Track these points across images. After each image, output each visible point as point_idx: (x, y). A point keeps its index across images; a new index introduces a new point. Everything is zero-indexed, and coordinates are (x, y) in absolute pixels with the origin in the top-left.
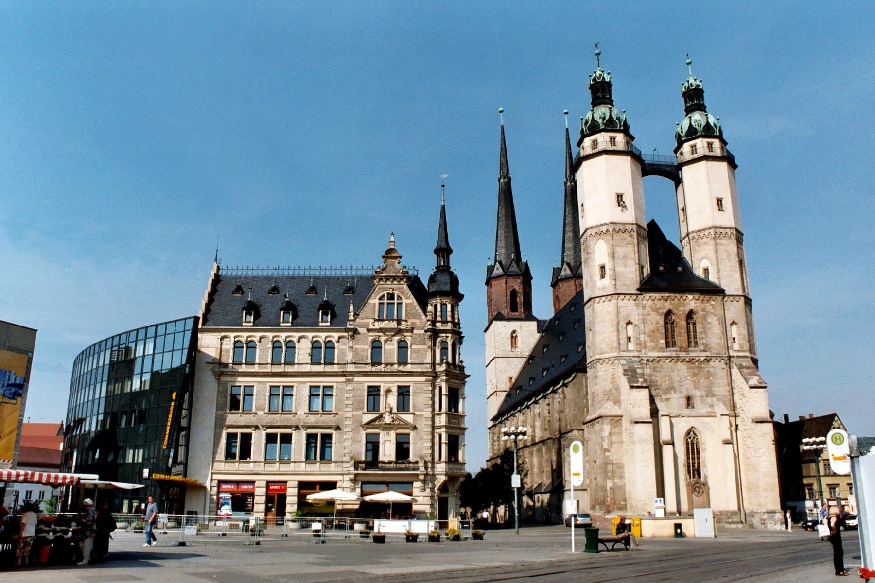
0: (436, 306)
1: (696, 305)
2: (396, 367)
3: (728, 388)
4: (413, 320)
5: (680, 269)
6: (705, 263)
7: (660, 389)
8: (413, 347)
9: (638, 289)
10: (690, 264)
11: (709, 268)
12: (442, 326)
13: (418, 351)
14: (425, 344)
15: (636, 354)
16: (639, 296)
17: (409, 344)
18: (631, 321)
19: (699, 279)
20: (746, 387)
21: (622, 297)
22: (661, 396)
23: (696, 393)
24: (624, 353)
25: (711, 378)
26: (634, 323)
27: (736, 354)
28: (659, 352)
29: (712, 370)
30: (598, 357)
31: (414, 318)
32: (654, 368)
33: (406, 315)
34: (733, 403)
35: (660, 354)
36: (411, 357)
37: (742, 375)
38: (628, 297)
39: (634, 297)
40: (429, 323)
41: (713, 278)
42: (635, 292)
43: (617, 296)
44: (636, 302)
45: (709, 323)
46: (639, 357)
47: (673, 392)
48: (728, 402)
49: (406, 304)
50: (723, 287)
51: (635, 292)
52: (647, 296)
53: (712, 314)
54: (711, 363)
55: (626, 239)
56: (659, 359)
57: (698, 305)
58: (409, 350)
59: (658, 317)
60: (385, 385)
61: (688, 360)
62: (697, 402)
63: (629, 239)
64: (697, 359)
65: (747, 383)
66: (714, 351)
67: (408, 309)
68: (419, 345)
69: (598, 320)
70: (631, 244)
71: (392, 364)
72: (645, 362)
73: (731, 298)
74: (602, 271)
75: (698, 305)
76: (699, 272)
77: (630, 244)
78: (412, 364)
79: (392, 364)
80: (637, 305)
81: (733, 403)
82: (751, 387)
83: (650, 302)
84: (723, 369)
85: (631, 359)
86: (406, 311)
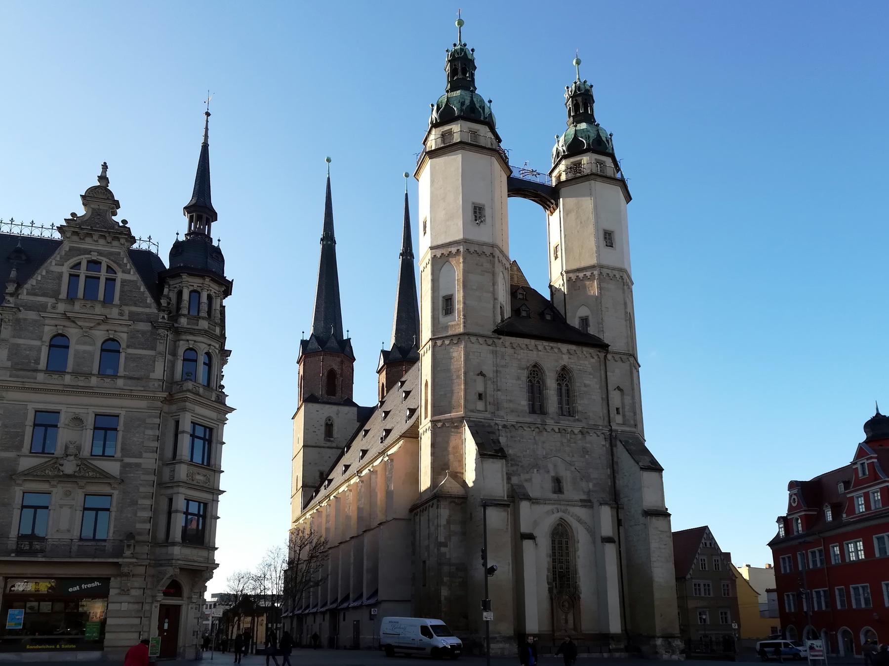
0: (180, 294)
1: (570, 361)
2: (94, 381)
3: (609, 471)
4: (134, 309)
5: (548, 317)
6: (583, 312)
7: (518, 465)
8: (130, 351)
9: (495, 332)
10: (562, 313)
11: (590, 319)
12: (188, 324)
13: (140, 357)
14: (153, 348)
15: (488, 415)
16: (496, 340)
17: (123, 345)
18: (484, 372)
19: (573, 329)
20: (637, 468)
21: (473, 339)
22: (520, 475)
23: (566, 476)
24: (472, 414)
25: (587, 456)
26: (487, 375)
27: (620, 429)
28: (519, 416)
29: (588, 445)
30: (436, 418)
31: (135, 305)
32: (511, 437)
33: (120, 299)
34: (615, 493)
35: (521, 419)
36: (125, 368)
37: (629, 453)
38: (481, 340)
39: (490, 341)
40: (161, 314)
41: (592, 330)
42: (490, 333)
43: (467, 337)
44: (491, 348)
45: (585, 386)
46: (493, 420)
47: (535, 470)
48: (608, 489)
49: (123, 282)
50: (606, 341)
51: (490, 333)
52: (508, 340)
53: (590, 374)
54: (588, 438)
55: (482, 265)
56: (521, 425)
57: (573, 361)
58: (123, 356)
59: (519, 371)
60: (70, 410)
61: (557, 430)
62: (567, 486)
63: (487, 266)
64: (569, 430)
65: (638, 464)
66: (591, 422)
67: (126, 288)
68: (143, 349)
69: (439, 369)
70: (489, 272)
71: (88, 375)
72: (500, 427)
73: (617, 357)
74: (447, 305)
75: (573, 361)
76: (575, 322)
77: (487, 272)
78: (124, 377)
79: (88, 375)
80: (495, 353)
81: (615, 491)
82: (641, 468)
83: (510, 351)
84: (603, 445)
85: (481, 422)
86: (122, 291)
